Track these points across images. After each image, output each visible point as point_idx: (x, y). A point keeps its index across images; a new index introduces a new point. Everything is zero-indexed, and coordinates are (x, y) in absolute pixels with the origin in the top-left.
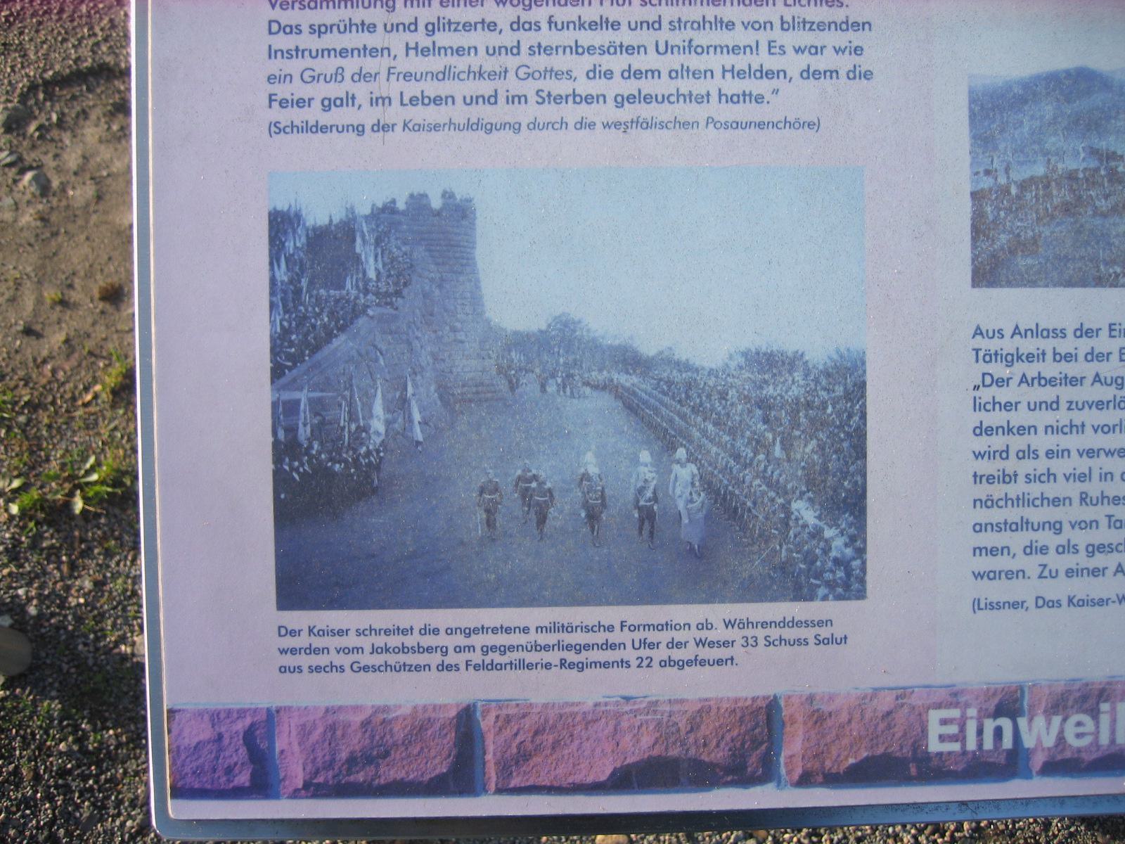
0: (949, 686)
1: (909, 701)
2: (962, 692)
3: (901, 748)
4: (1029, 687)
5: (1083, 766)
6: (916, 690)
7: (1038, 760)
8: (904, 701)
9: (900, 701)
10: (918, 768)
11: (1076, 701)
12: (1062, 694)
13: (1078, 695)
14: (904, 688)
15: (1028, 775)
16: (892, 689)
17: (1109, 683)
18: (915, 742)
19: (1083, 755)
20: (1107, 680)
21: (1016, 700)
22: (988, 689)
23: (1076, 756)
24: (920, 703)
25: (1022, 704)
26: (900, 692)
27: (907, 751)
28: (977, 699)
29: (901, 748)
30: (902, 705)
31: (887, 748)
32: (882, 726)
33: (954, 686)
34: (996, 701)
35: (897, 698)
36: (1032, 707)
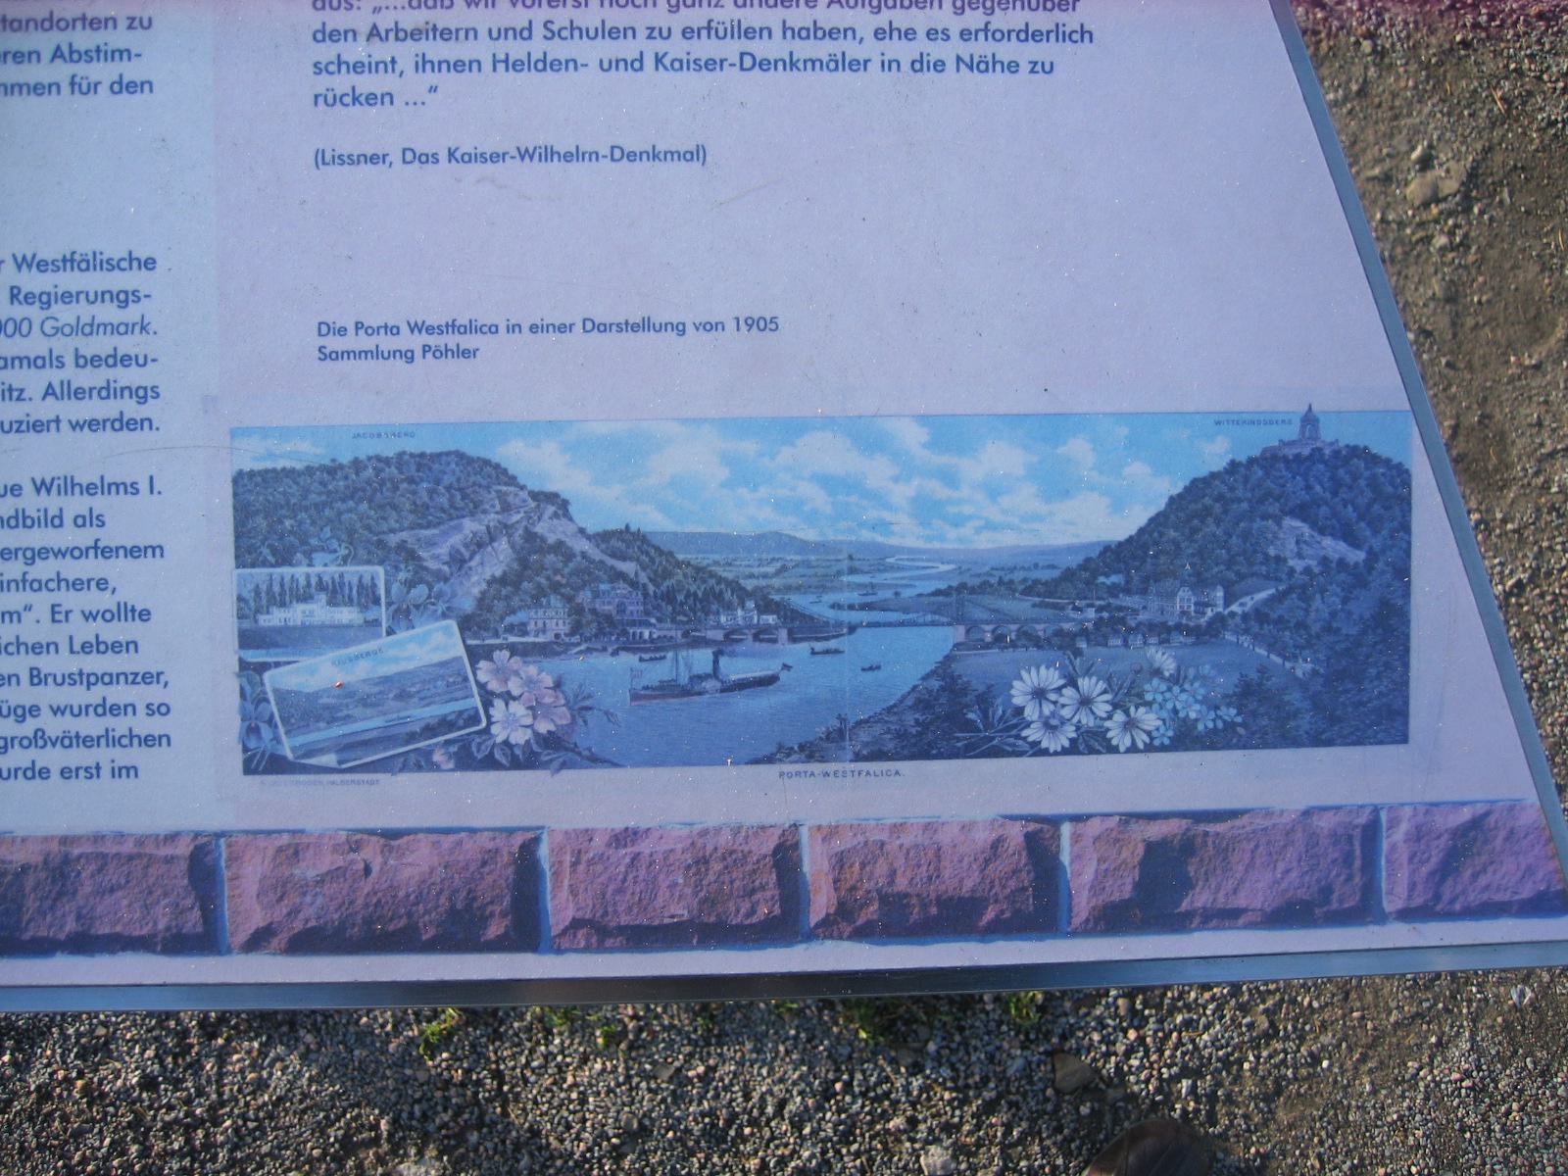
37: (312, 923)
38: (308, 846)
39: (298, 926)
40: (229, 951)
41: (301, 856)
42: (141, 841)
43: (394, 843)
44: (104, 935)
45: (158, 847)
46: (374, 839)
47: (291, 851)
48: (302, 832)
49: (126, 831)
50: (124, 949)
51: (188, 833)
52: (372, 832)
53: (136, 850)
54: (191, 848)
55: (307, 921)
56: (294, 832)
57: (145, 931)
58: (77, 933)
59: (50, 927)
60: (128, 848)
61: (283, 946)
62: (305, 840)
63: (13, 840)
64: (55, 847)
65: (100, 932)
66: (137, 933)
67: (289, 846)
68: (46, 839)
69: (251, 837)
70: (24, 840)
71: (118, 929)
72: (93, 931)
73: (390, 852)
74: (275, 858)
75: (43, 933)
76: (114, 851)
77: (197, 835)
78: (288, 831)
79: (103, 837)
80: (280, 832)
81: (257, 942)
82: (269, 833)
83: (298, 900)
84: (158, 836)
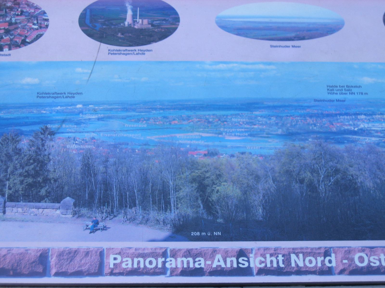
0: (24, 248)
1: (12, 252)
2: (29, 250)
3: (8, 266)
4: (52, 249)
5: (69, 274)
6: (14, 249)
7: (54, 271)
8: (10, 252)
9: (9, 252)
10: (13, 272)
11: (67, 254)
12: (62, 252)
13: (67, 252)
14: (11, 248)
15: (50, 276)
16: (6, 248)
17: (78, 249)
18: (12, 265)
19: (69, 271)
20: (78, 248)
21: (47, 253)
22: (38, 249)
23: (66, 271)
24: (15, 252)
25: (49, 254)
26: (9, 249)
27: (10, 267)
28: (34, 252)
29: (8, 266)
30: (9, 253)
31: (3, 266)
32: (2, 259)
33: (27, 248)
34: (40, 253)
35: (8, 251)
36: (51, 255)
37: (355, 268)
38: (352, 250)
39: (351, 268)
40: (335, 274)
41: (351, 252)
42: (312, 249)
43: (373, 250)
44: (305, 271)
45: (316, 250)
46: (368, 249)
47: (348, 251)
48: (350, 247)
49: (308, 247)
50: (309, 274)
51: (323, 247)
52: (367, 247)
53: (311, 251)
54: (324, 250)
55: (353, 267)
56: (349, 247)
57: (314, 270)
58: (297, 270)
59: (290, 269)
60: (309, 250)
61: (348, 273)
62: (351, 249)
63: (281, 249)
64: (291, 250)
65: (303, 270)
66: (311, 270)
67: (348, 250)
68: (289, 248)
69: (338, 248)
70: (284, 249)
71: (307, 269)
72: (301, 270)
73: (372, 251)
74: (344, 253)
75: (289, 270)
76: (306, 251)
77: (325, 248)
78: (347, 247)
79: (303, 248)
80: (345, 247)
81: (342, 272)
82: (343, 247)
83: (351, 263)
84: (316, 248)
